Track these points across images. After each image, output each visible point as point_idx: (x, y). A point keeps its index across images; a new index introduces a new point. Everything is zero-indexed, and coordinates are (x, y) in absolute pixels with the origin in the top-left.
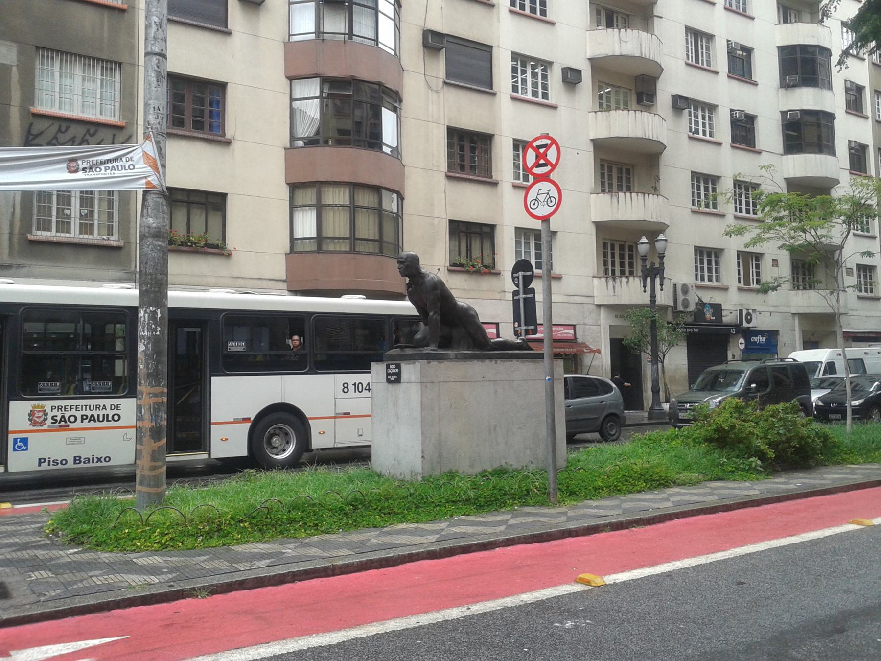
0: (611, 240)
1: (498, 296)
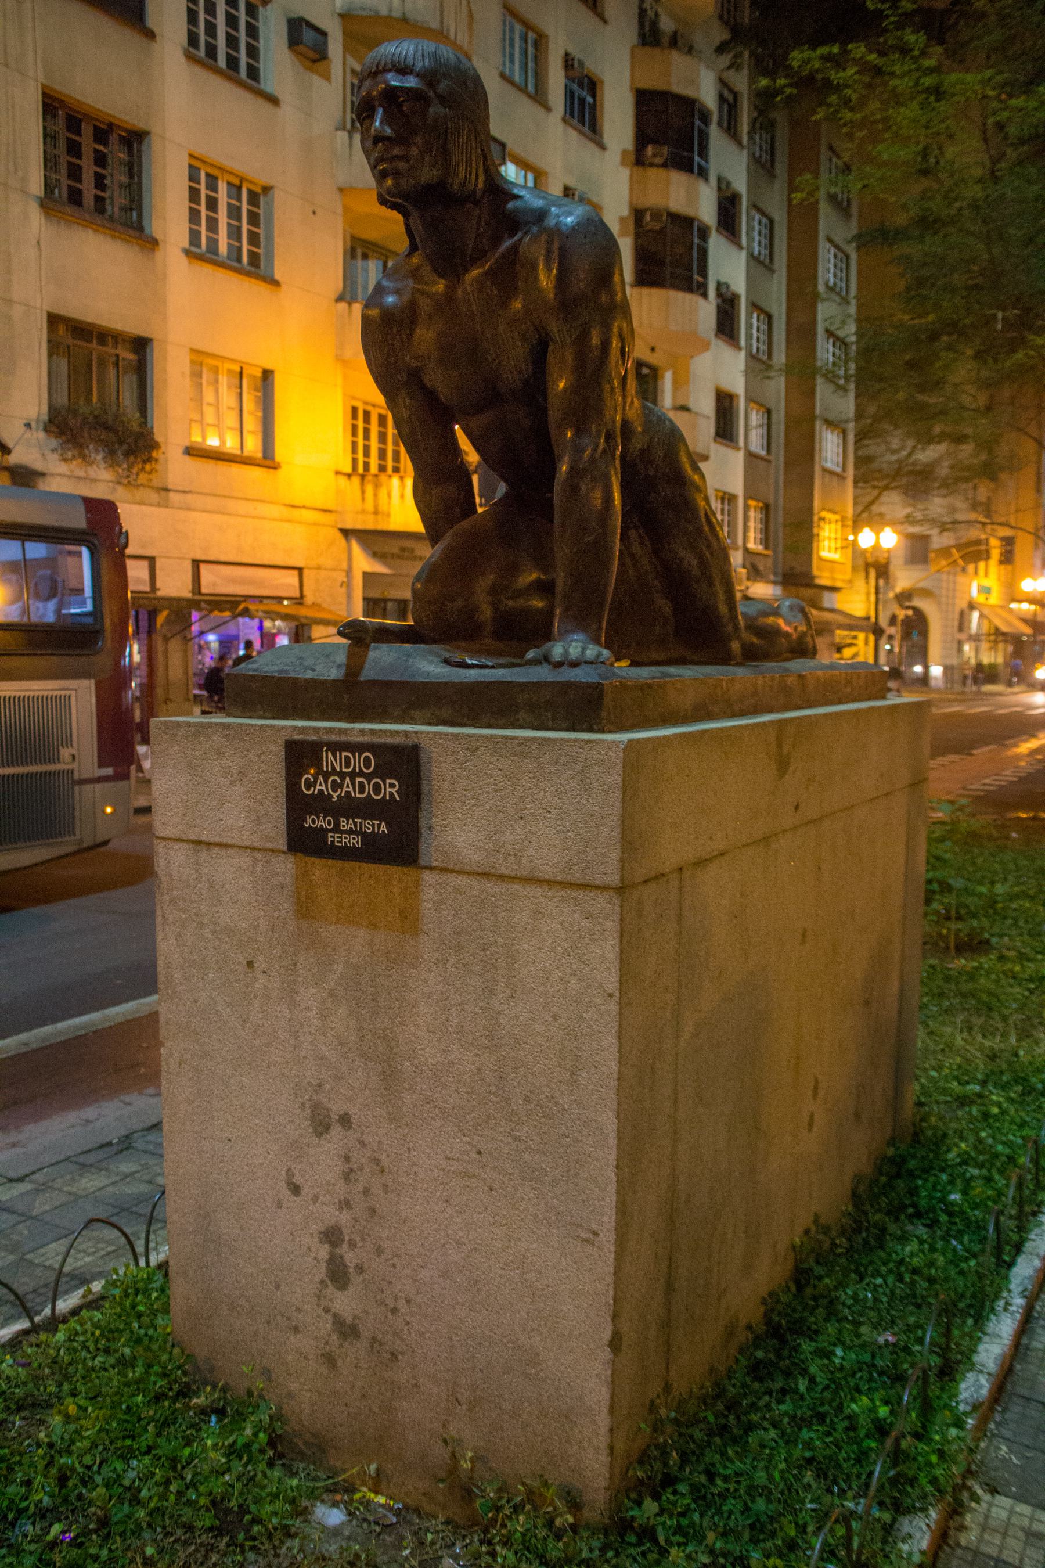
0: (366, 403)
1: (154, 497)
